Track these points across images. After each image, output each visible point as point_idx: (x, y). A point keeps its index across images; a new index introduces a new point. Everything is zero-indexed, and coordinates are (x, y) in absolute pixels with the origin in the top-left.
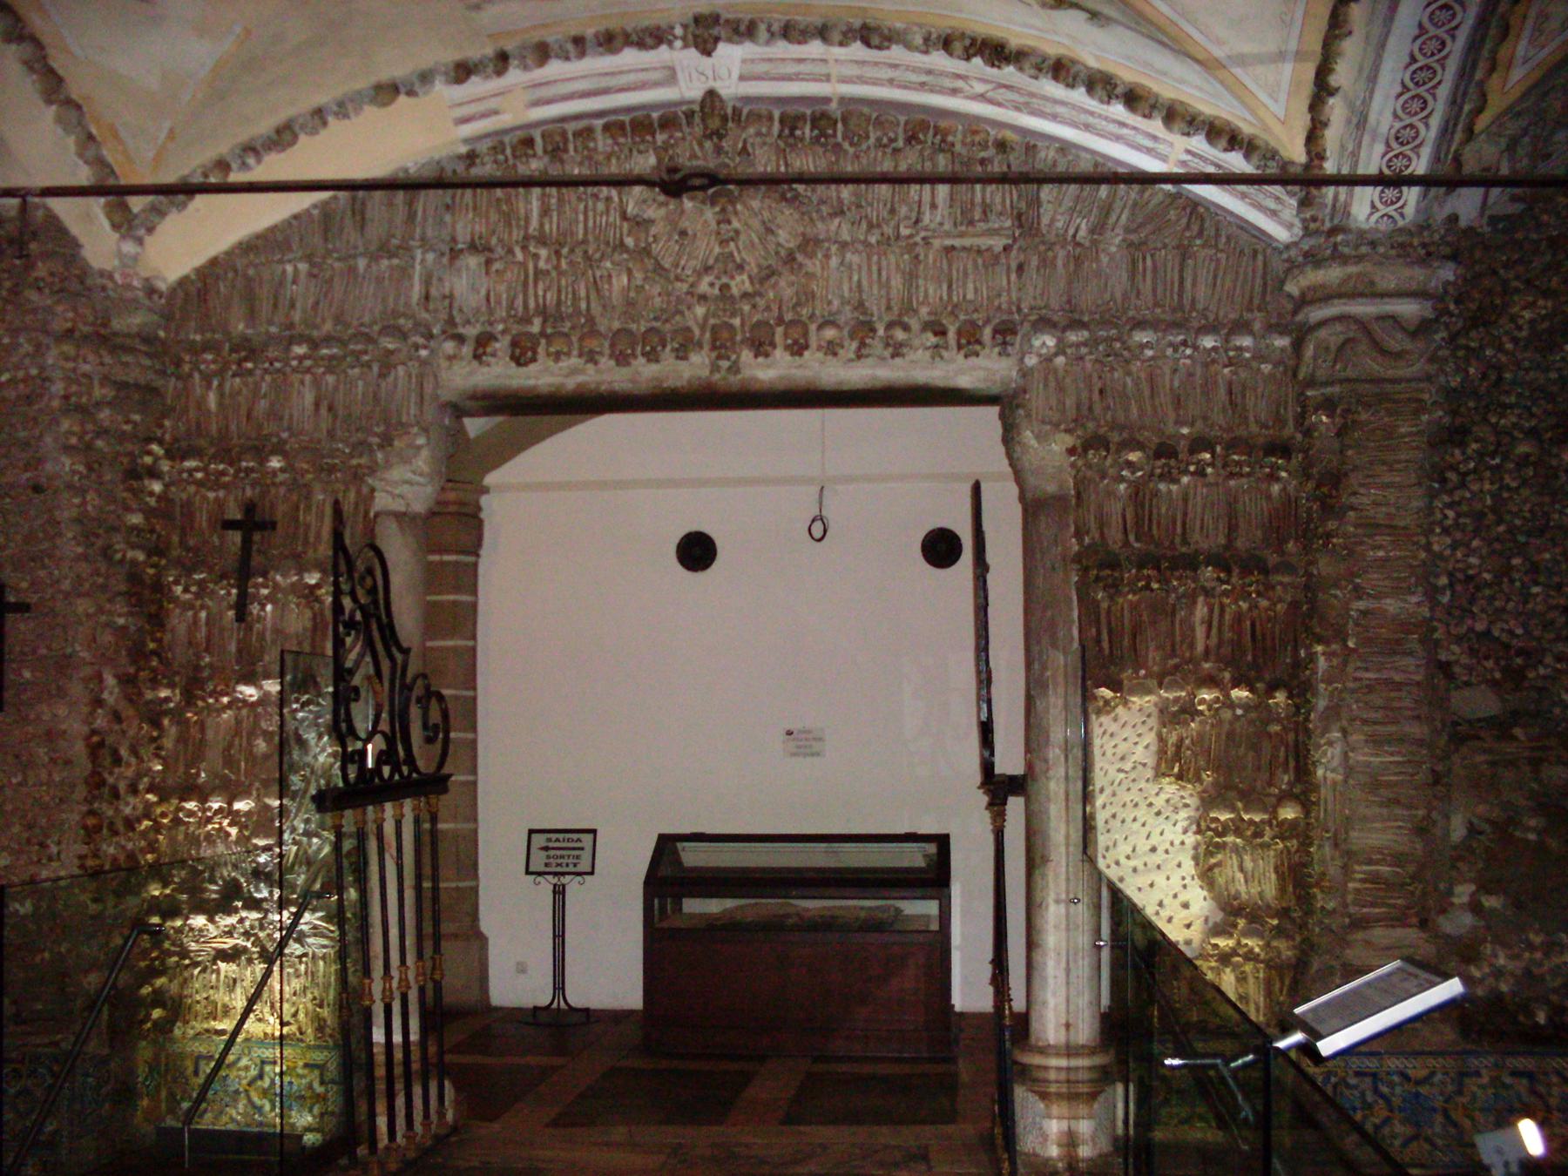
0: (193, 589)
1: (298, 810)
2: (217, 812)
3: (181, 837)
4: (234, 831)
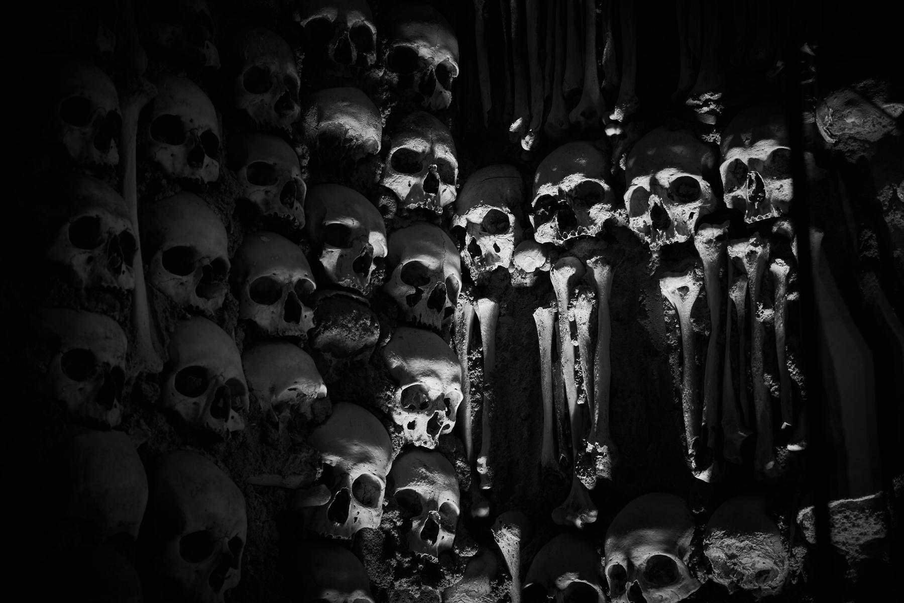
0: (546, 233)
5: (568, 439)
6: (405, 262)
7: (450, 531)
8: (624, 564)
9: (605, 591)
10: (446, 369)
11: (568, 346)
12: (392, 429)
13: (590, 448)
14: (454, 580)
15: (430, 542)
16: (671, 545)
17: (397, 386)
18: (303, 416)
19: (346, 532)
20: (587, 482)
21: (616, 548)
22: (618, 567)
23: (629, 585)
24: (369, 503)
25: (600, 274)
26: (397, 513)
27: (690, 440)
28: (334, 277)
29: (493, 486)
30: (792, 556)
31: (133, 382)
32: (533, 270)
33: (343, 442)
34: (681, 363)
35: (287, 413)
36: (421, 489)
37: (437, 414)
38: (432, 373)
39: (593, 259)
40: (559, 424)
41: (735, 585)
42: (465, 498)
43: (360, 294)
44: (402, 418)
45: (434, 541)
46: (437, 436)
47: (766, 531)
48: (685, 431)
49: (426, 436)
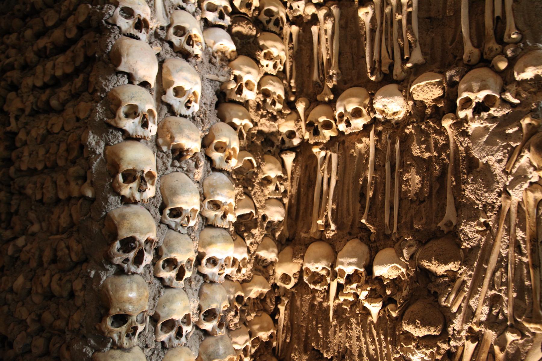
1: (478, 281)
2: (350, 279)
3: (306, 309)
4: (375, 308)
5: (323, 71)
6: (266, 8)
7: (280, 102)
8: (343, 111)
9: (336, 123)
10: (280, 46)
11: (323, 38)
12: (260, 66)
13: (331, 74)
14: (281, 121)
15: (273, 106)
16: (361, 103)
17: (262, 50)
18: (226, 57)
19: (242, 99)
20: (330, 85)
21: (341, 105)
22: (341, 113)
23: (345, 118)
24: (251, 90)
25: (335, 10)
26: (261, 95)
27: (368, 66)
28: (239, 9)
29: (297, 90)
30: (408, 104)
31: (154, 28)
32: (311, 13)
33: (241, 66)
34: (366, 40)
35: (220, 54)
36: (270, 88)
37: (276, 62)
38: (275, 47)
39: (333, 6)
40: (320, 66)
41: (385, 118)
42: (286, 93)
43: (247, 15)
44: (264, 62)
45: (275, 106)
46: (277, 70)
47: (398, 96)
48: (366, 63)
49: (272, 69)
